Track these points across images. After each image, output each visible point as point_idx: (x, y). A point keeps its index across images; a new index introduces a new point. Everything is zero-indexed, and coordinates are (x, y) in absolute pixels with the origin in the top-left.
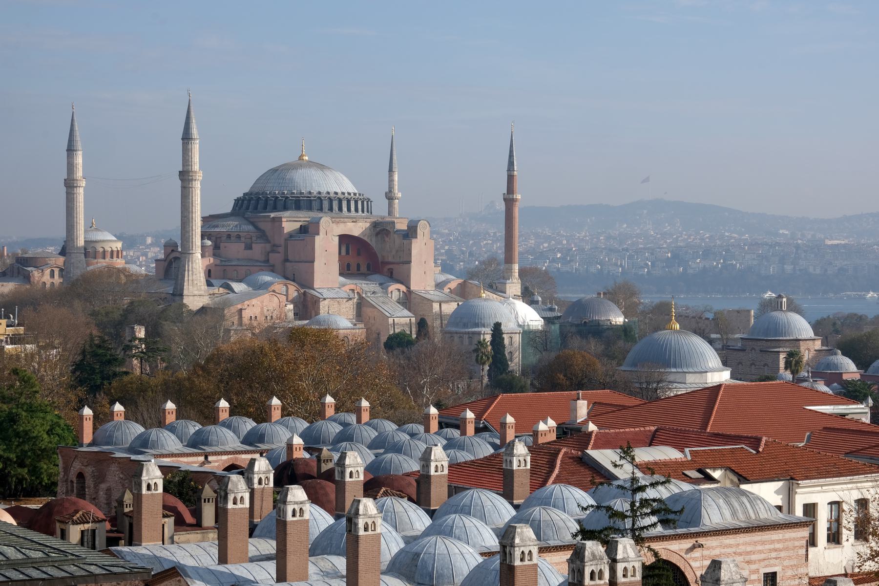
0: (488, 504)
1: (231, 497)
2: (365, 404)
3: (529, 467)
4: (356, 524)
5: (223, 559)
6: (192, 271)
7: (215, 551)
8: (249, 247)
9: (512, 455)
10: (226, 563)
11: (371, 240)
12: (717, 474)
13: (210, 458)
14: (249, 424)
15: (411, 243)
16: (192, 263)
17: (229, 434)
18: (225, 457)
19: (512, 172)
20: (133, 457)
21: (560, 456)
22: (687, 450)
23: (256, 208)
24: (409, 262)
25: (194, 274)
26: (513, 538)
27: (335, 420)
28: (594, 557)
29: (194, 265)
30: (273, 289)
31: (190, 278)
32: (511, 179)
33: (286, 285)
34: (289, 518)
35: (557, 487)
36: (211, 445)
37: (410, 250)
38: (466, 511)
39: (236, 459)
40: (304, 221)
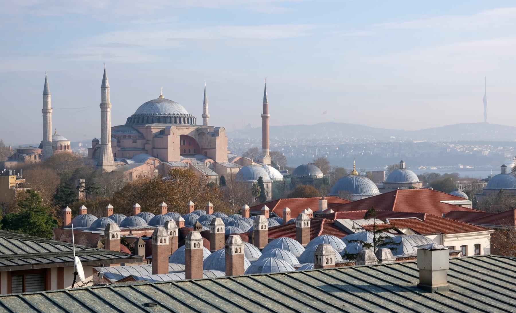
0: (291, 245)
1: (159, 239)
2: (210, 205)
3: (309, 226)
4: (231, 249)
5: (155, 272)
6: (107, 153)
7: (150, 270)
8: (135, 142)
9: (301, 220)
10: (157, 274)
11: (196, 137)
12: (404, 231)
13: (133, 232)
14: (151, 216)
15: (216, 139)
16: (107, 150)
17: (142, 220)
18: (140, 232)
19: (266, 103)
20: (93, 232)
21: (323, 222)
22: (387, 219)
23: (138, 122)
24: (215, 148)
25: (108, 155)
26: (322, 251)
27: (195, 213)
28: (370, 258)
29: (108, 150)
30: (147, 162)
31: (106, 157)
32: (265, 106)
33: (154, 160)
34: (192, 248)
35: (325, 236)
36: (133, 226)
37: (215, 142)
38: (280, 247)
39: (146, 233)
40: (162, 128)
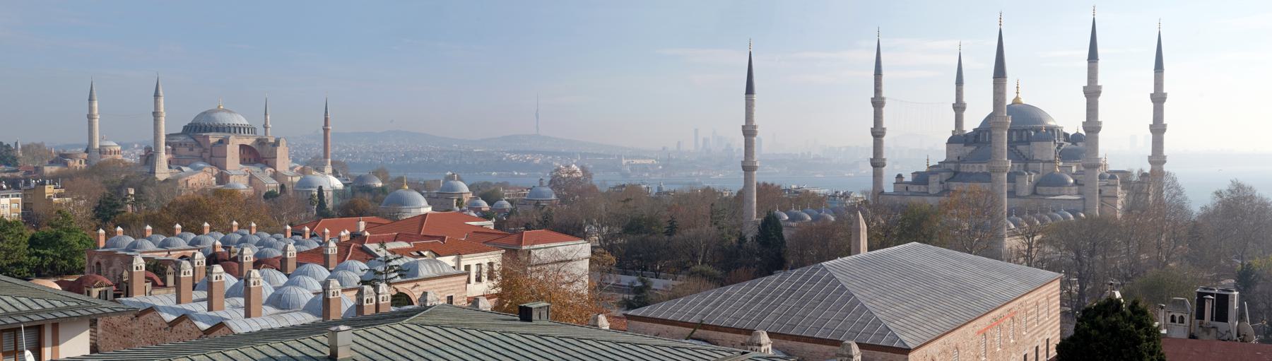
0: (316, 270)
1: (182, 272)
2: (254, 225)
3: (336, 252)
4: (249, 282)
5: (178, 302)
7: (174, 298)
8: (191, 150)
10: (180, 303)
12: (425, 253)
13: (171, 253)
14: (192, 236)
17: (181, 241)
18: (179, 252)
20: (128, 253)
21: (352, 247)
22: (412, 243)
24: (276, 158)
26: (329, 286)
27: (238, 233)
28: (368, 292)
32: (326, 120)
34: (214, 280)
35: (350, 261)
37: (276, 152)
38: (306, 274)
